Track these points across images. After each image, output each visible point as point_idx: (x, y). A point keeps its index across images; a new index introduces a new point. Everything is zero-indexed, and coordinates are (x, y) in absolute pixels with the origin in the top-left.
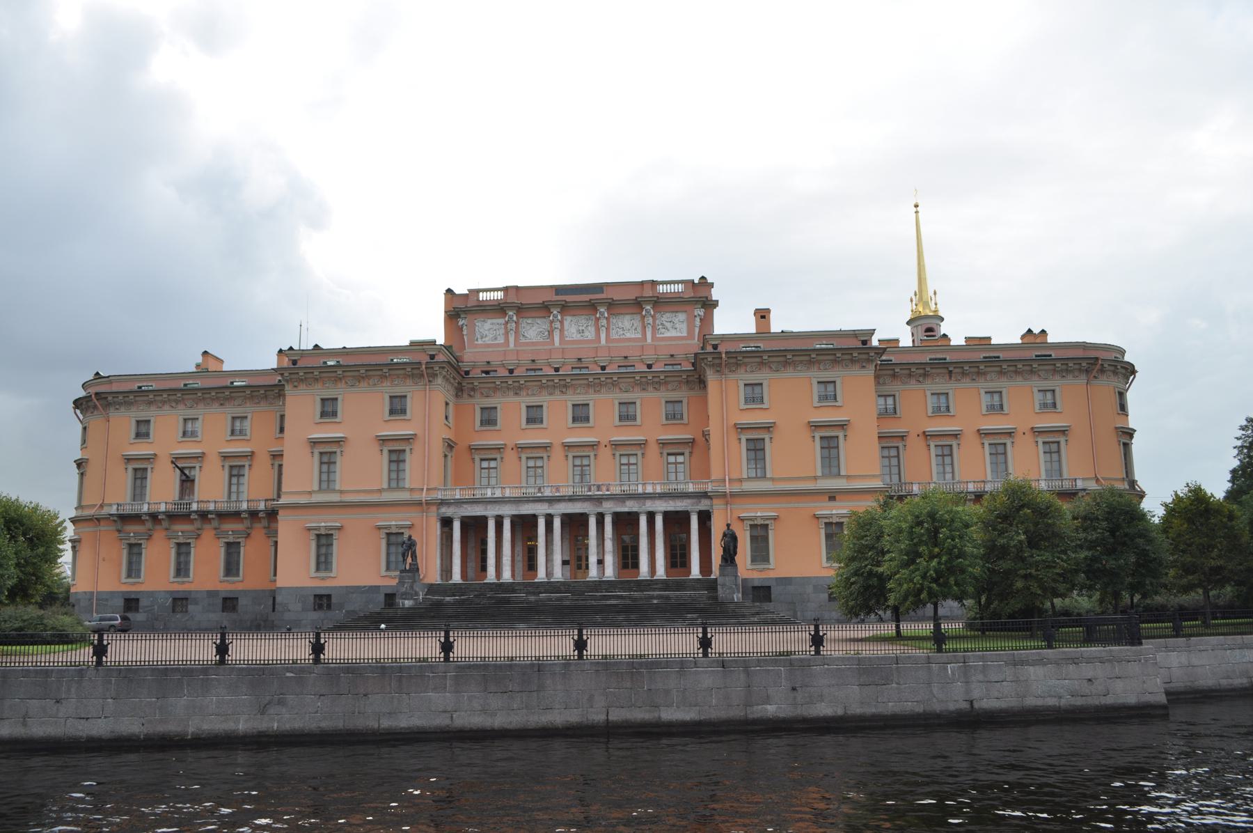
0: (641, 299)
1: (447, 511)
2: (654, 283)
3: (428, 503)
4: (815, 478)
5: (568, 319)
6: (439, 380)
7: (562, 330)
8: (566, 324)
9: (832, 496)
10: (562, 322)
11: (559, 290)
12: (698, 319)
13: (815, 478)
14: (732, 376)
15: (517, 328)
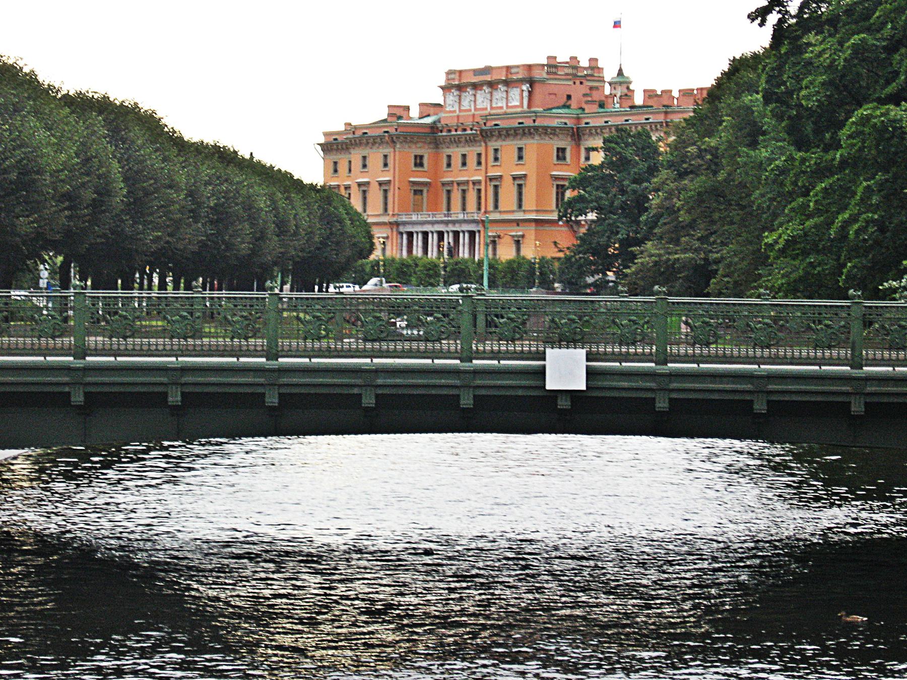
0: (507, 79)
1: (402, 229)
2: (508, 68)
3: (390, 223)
4: (513, 212)
5: (479, 92)
6: (398, 146)
7: (475, 101)
8: (478, 96)
9: (518, 222)
10: (475, 95)
11: (477, 72)
12: (526, 94)
13: (513, 212)
14: (489, 144)
15: (460, 100)
